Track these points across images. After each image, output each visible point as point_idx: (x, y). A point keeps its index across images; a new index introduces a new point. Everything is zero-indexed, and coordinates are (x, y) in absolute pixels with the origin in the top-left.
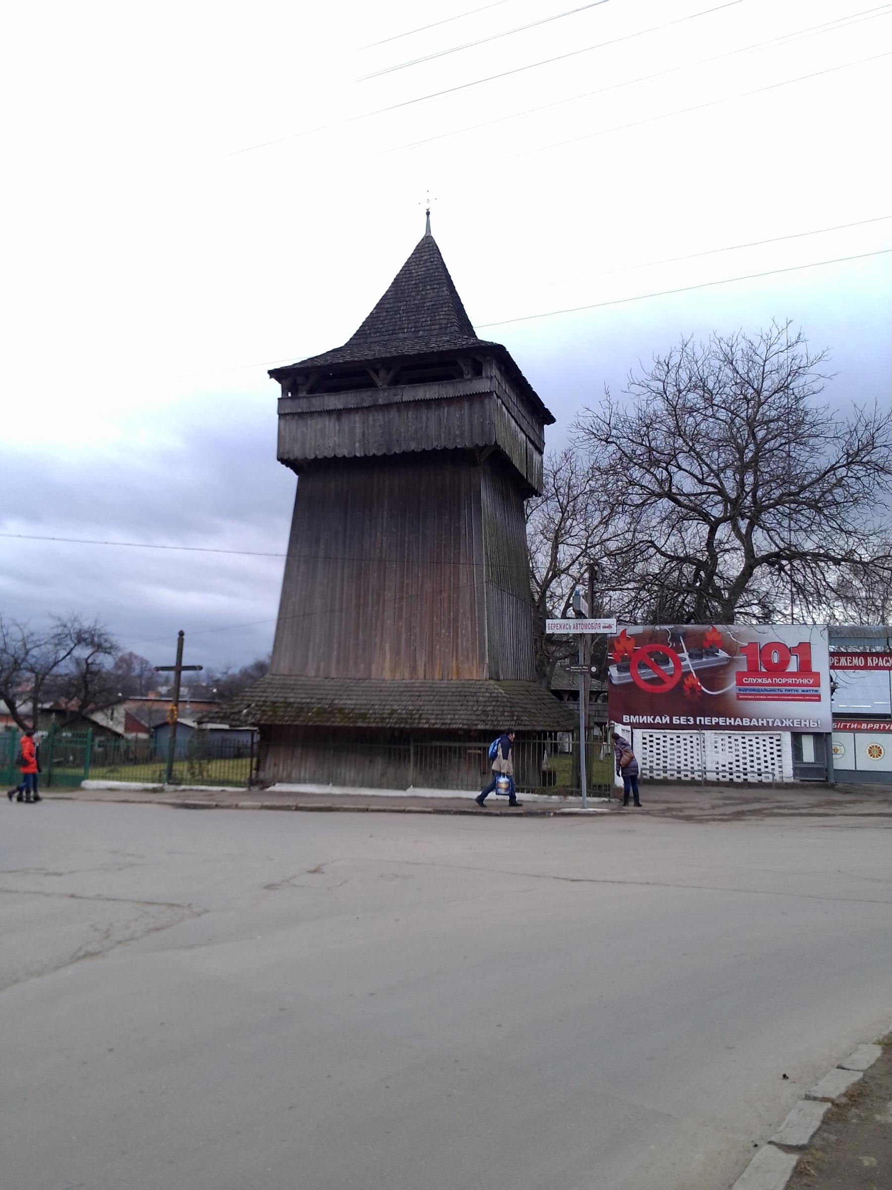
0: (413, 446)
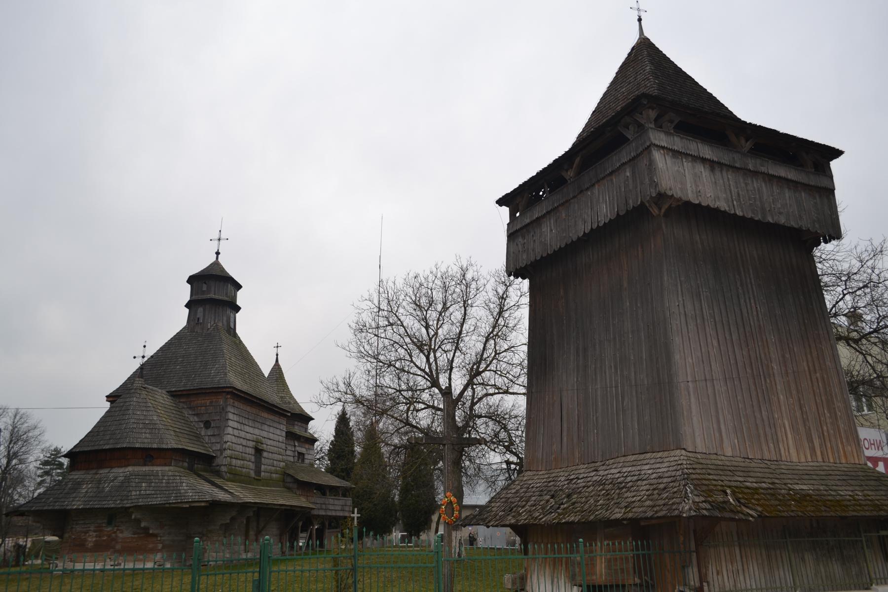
0: (782, 220)
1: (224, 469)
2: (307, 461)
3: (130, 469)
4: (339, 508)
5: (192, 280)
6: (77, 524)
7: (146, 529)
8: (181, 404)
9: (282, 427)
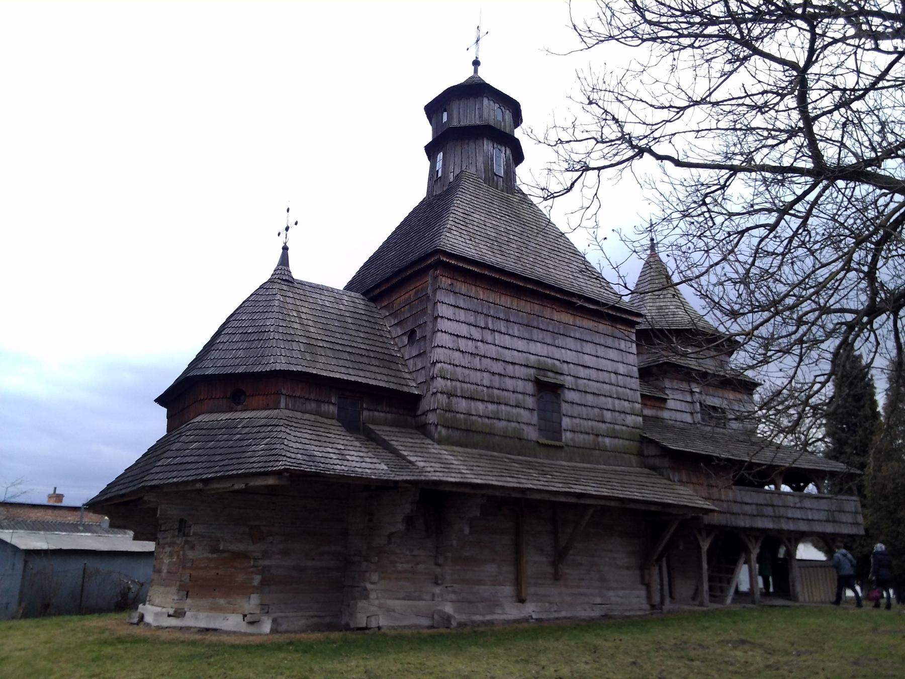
1: (432, 418)
4: (822, 516)
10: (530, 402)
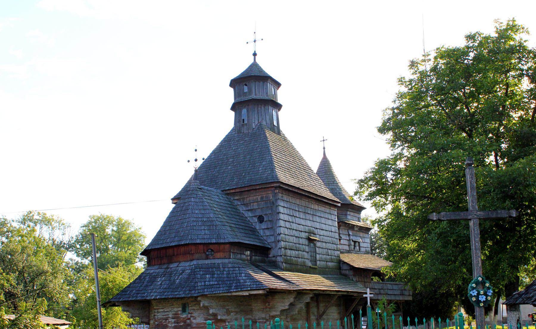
1: (279, 259)
2: (363, 249)
3: (195, 262)
5: (234, 83)
6: (158, 312)
7: (215, 315)
8: (236, 202)
9: (333, 217)
10: (307, 249)
